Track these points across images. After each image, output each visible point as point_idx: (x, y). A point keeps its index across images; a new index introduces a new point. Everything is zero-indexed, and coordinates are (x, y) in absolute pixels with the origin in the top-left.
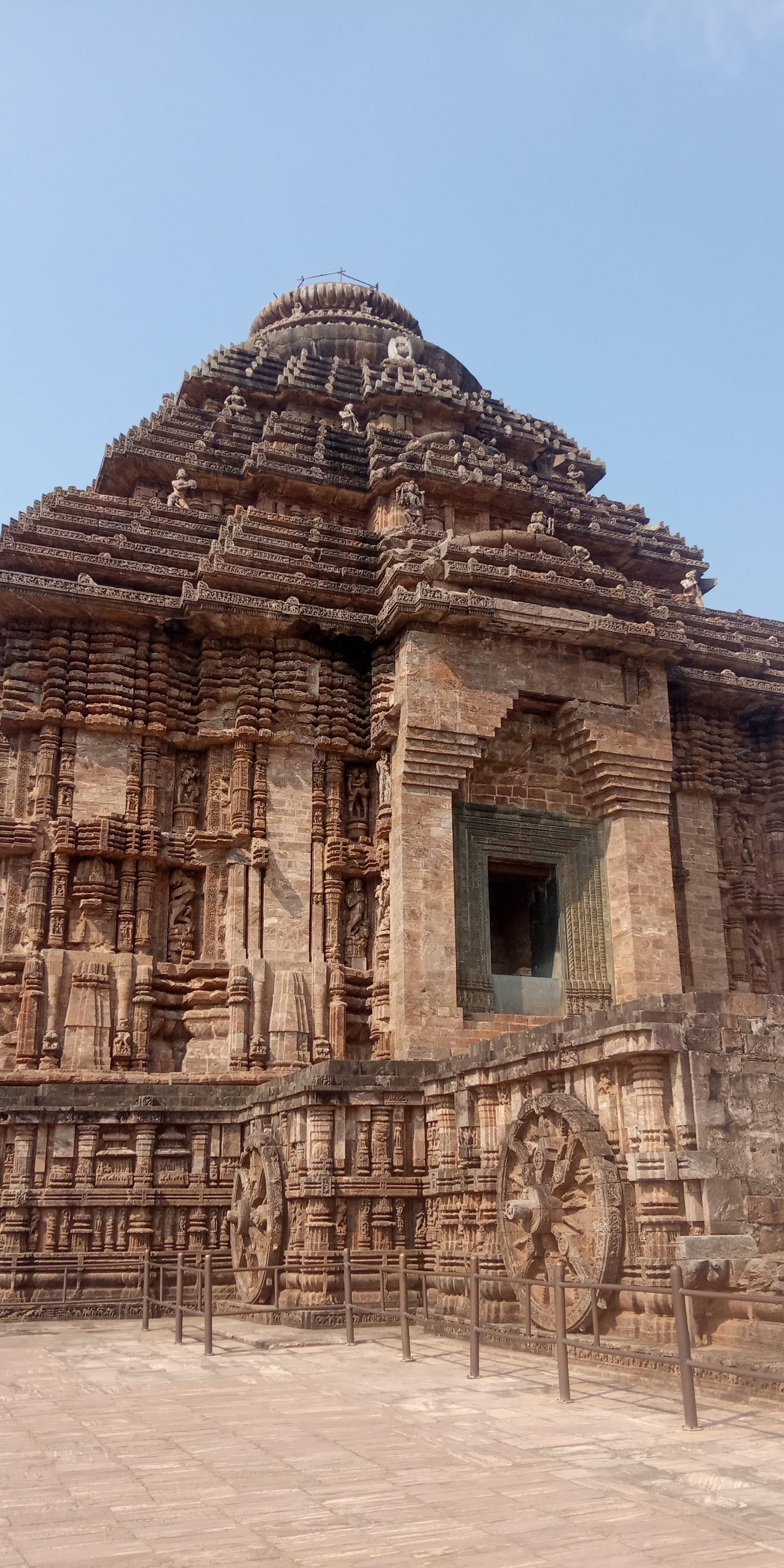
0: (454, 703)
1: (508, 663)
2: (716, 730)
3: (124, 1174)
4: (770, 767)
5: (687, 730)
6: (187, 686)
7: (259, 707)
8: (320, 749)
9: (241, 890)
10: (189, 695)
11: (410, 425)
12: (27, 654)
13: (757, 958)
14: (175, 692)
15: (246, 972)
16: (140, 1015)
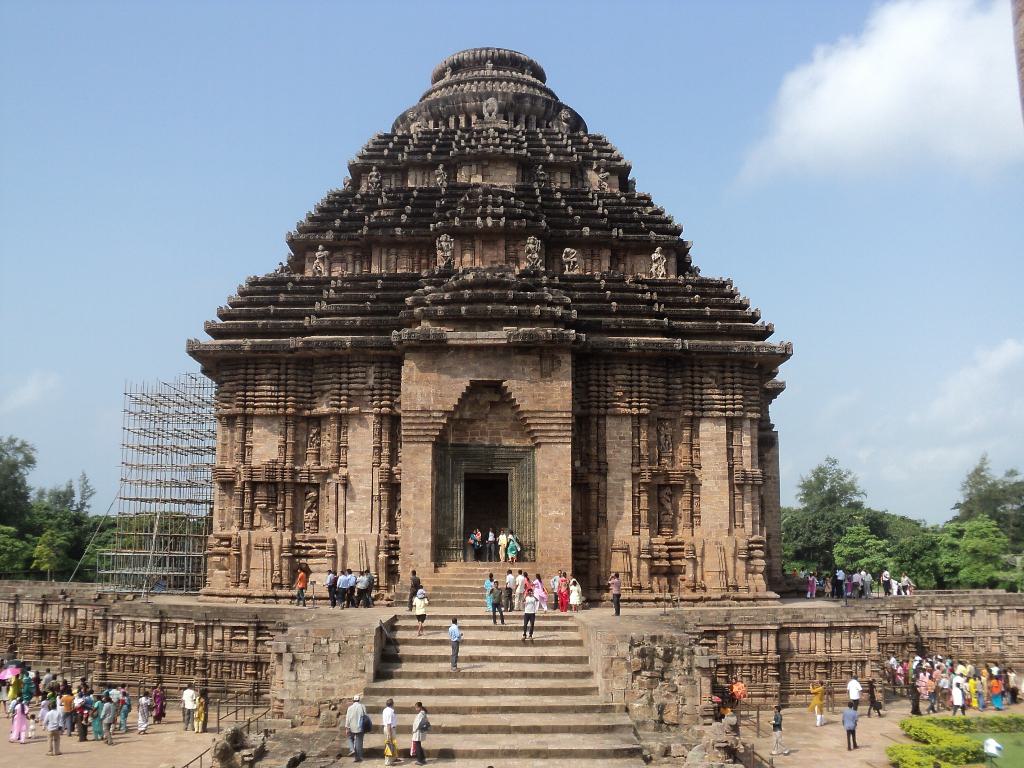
0: (428, 395)
1: (463, 364)
2: (635, 372)
3: (243, 647)
4: (684, 388)
5: (613, 375)
6: (309, 384)
7: (340, 395)
8: (377, 415)
9: (333, 497)
10: (309, 390)
11: (480, 171)
12: (228, 378)
13: (667, 510)
14: (301, 389)
15: (334, 541)
16: (285, 563)
